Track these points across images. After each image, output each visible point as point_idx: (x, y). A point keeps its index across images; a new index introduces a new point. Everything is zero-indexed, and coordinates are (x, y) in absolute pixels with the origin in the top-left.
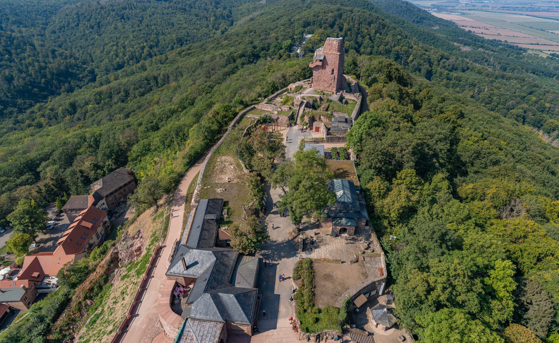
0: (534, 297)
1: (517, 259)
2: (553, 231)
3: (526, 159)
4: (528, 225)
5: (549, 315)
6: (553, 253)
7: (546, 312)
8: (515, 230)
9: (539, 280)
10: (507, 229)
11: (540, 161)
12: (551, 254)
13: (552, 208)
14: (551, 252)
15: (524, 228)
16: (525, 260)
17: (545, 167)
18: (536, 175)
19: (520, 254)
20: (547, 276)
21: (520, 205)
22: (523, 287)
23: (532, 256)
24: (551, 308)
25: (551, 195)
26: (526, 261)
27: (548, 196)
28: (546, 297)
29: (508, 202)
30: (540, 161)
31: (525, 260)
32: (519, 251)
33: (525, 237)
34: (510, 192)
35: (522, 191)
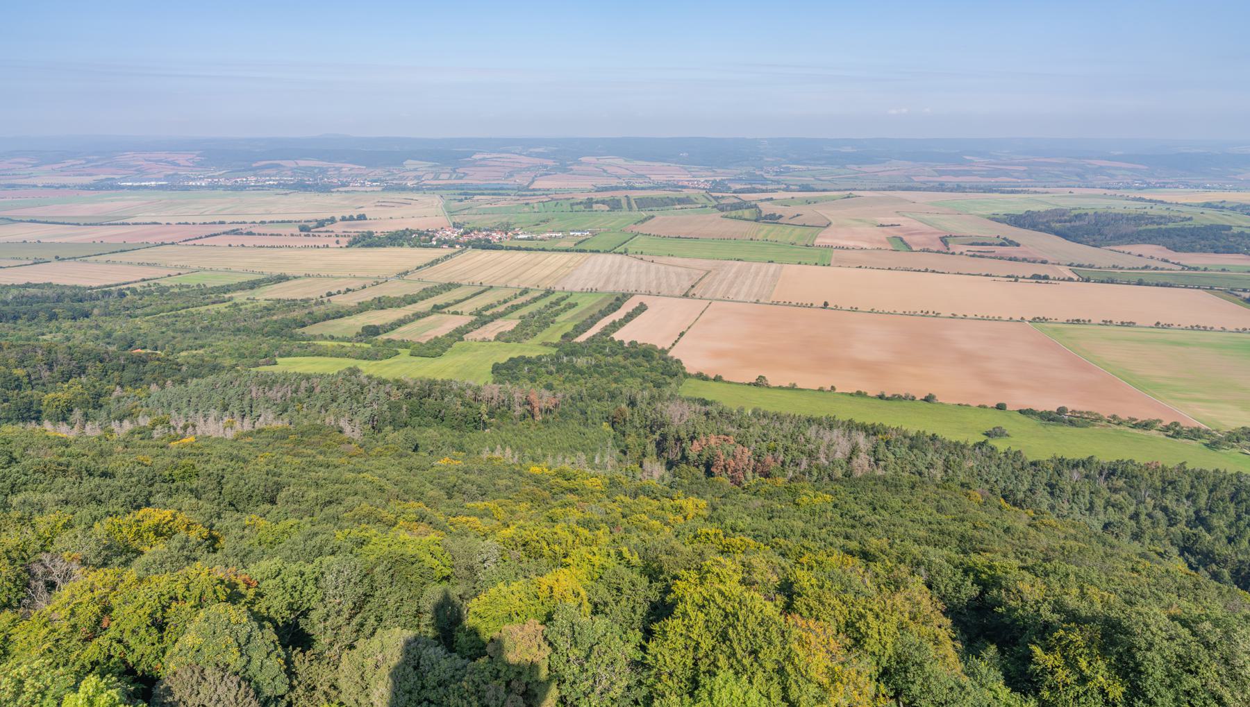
0: (201, 695)
1: (124, 662)
2: (154, 561)
3: (24, 478)
4: (93, 584)
5: (248, 700)
6: (172, 594)
7: (240, 700)
8: (73, 613)
9: (184, 659)
10: (56, 625)
11: (62, 468)
12: (171, 598)
13: (134, 529)
14: (167, 596)
15: (89, 595)
16: (140, 649)
17: (80, 473)
18: (69, 494)
19: (120, 648)
20: (190, 640)
21: (59, 564)
22: (170, 699)
23: (142, 632)
24: (240, 686)
25: (121, 510)
26: (142, 651)
27: (117, 513)
28: (218, 675)
29: (26, 576)
30: (60, 468)
31: (140, 649)
32: (114, 644)
33: (107, 610)
34: (14, 555)
35: (47, 535)
